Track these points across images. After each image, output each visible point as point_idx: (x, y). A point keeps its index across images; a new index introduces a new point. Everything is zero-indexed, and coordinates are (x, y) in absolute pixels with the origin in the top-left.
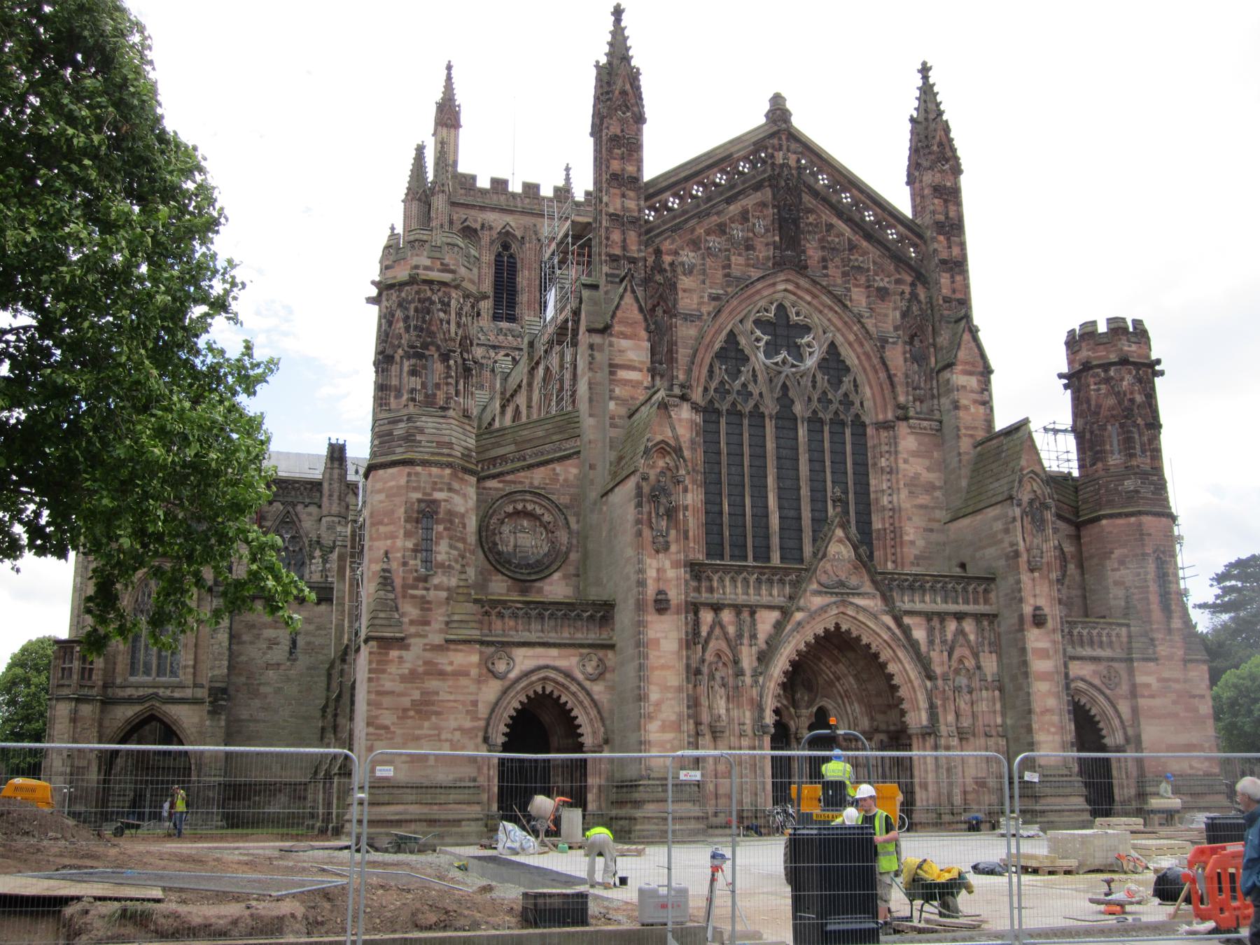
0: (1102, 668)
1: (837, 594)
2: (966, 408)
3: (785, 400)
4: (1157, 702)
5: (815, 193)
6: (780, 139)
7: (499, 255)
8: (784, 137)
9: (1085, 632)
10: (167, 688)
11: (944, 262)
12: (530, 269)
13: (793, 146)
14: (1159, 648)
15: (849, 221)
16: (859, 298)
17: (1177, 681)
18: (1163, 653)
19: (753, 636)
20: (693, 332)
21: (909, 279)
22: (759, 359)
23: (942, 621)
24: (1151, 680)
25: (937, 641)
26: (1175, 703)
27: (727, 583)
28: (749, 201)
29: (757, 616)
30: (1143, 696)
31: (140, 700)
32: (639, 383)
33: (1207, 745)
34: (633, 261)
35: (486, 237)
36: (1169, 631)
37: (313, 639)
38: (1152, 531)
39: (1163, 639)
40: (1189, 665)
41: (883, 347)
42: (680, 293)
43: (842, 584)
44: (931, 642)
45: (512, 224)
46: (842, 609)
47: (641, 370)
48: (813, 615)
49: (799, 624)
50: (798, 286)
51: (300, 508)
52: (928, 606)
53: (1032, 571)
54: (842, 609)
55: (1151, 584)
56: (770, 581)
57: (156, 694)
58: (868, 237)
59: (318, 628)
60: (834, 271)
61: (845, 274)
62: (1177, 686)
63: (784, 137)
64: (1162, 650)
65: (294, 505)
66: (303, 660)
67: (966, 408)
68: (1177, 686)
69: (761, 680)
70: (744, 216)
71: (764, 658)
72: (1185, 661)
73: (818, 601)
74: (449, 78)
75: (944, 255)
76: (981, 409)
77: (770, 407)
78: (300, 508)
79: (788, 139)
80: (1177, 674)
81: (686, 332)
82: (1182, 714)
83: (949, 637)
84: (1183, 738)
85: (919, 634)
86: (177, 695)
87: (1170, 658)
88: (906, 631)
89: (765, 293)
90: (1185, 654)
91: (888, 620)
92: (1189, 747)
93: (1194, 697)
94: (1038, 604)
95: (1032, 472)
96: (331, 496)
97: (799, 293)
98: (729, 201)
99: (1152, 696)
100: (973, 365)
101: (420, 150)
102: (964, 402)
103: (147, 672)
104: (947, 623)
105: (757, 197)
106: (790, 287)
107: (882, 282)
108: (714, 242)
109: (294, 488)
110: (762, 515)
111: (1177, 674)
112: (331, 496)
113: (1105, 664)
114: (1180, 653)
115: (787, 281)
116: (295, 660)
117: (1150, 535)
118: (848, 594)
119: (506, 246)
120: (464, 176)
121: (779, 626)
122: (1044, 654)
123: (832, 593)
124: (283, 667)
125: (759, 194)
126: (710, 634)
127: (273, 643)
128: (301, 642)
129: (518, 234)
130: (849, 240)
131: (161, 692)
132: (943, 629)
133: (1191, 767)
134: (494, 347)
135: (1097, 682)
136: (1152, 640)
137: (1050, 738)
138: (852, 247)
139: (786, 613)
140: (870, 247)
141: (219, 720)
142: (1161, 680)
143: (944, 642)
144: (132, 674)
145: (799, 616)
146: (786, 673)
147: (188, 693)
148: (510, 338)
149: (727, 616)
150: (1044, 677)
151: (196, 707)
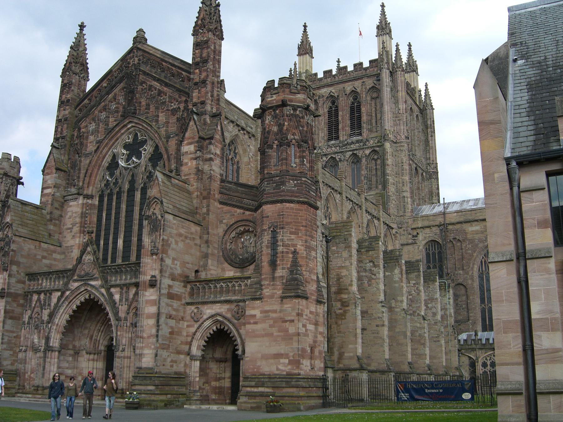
0: (233, 306)
1: (84, 280)
2: (187, 164)
3: (132, 182)
4: (259, 327)
5: (145, 73)
6: (134, 52)
7: (331, 108)
8: (135, 51)
9: (224, 285)
11: (196, 84)
12: (342, 111)
13: (140, 53)
14: (265, 291)
15: (158, 80)
16: (162, 118)
17: (275, 311)
18: (267, 294)
19: (49, 305)
20: (88, 162)
21: (184, 99)
22: (122, 163)
23: (128, 288)
24: (257, 312)
25: (124, 300)
26: (271, 326)
27: (45, 281)
28: (116, 90)
29: (53, 294)
30: (250, 323)
32: (50, 193)
33: (291, 354)
34: (63, 138)
36: (273, 279)
38: (269, 214)
39: (268, 284)
40: (284, 300)
41: (167, 141)
42: (89, 145)
43: (87, 274)
44: (121, 300)
45: (333, 91)
46: (86, 288)
47: (51, 188)
48: (73, 292)
49: (67, 298)
50: (136, 123)
52: (123, 282)
53: (152, 254)
54: (86, 288)
55: (264, 249)
56: (59, 278)
58: (167, 85)
60: (152, 108)
61: (157, 108)
62: (274, 315)
63: (135, 51)
64: (266, 292)
67: (187, 164)
68: (274, 315)
69: (50, 325)
70: (115, 98)
71: (51, 316)
72: (283, 298)
73: (76, 284)
74: (305, 31)
75: (197, 80)
76: (194, 162)
77: (127, 186)
79: (137, 52)
80: (276, 307)
81: (85, 162)
82: (275, 334)
83: (131, 296)
84: (274, 350)
85: (117, 297)
87: (272, 296)
88: (111, 295)
89: (122, 131)
90: (283, 293)
91: (103, 290)
92: (278, 356)
93: (286, 321)
94: (154, 274)
95: (155, 198)
97: (137, 126)
98: (108, 93)
99: (256, 323)
100: (193, 138)
102: (185, 161)
104: (130, 288)
105: (122, 85)
106: (133, 125)
107: (174, 106)
108: (103, 115)
110: (115, 243)
111: (276, 307)
113: (236, 304)
114: (279, 292)
115: (130, 122)
117: (268, 217)
118: (88, 280)
121: (59, 299)
122: (153, 303)
123: (81, 280)
125: (122, 84)
126: (35, 305)
129: (336, 95)
130: (159, 90)
132: (127, 292)
133: (278, 369)
135: (229, 315)
136: (262, 286)
137: (151, 351)
138: (160, 93)
139: (63, 293)
140: (168, 90)
142: (262, 312)
143: (127, 300)
145: (68, 293)
146: (68, 322)
148: (334, 148)
149: (42, 296)
150: (149, 316)
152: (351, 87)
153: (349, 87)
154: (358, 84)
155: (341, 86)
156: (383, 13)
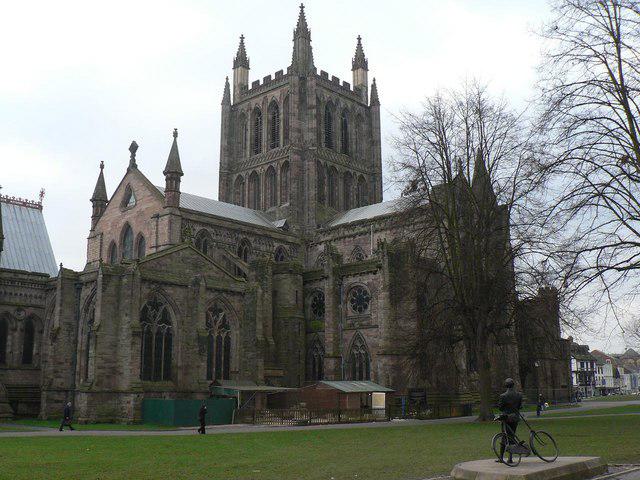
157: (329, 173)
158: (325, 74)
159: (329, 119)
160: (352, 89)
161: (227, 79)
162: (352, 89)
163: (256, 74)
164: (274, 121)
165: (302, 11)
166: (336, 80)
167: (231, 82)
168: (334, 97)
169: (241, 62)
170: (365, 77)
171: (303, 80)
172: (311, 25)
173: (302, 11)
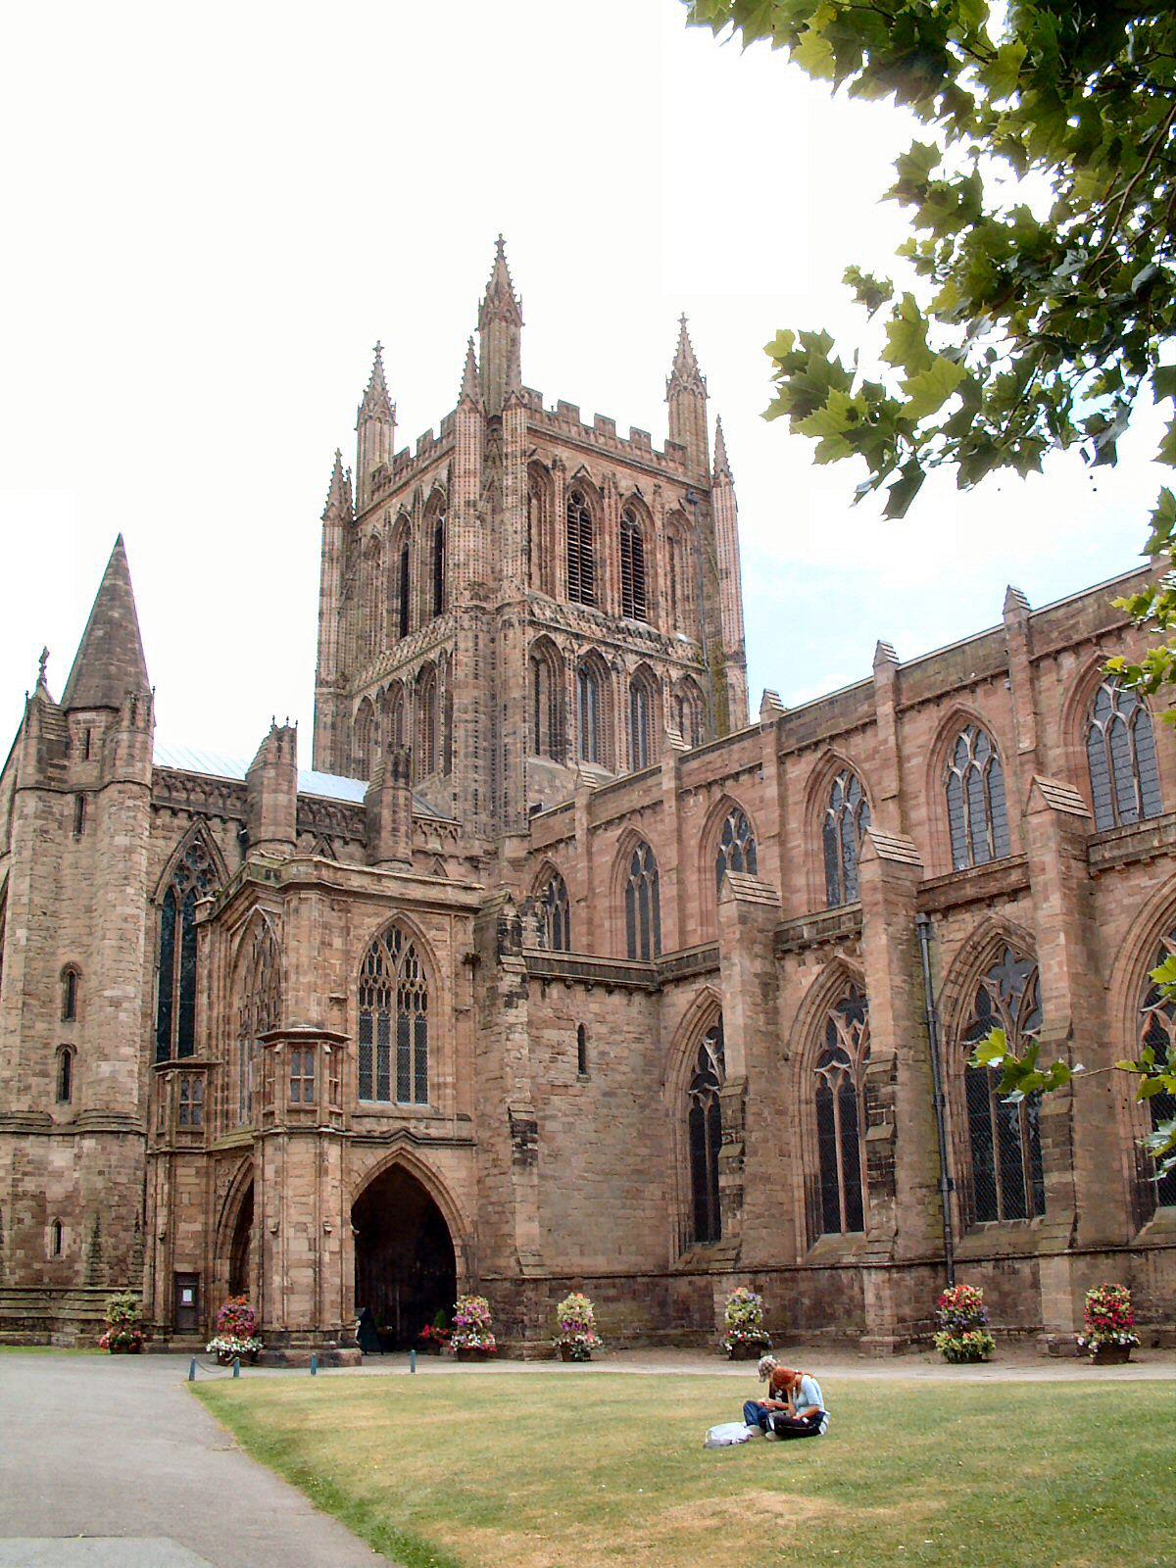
10: (419, 1120)
31: (384, 1140)
35: (558, 480)
37: (607, 1048)
45: (589, 469)
51: (337, 844)
57: (406, 1130)
59: (613, 1031)
65: (330, 838)
66: (597, 1081)
78: (337, 844)
86: (434, 1132)
96: (395, 830)
101: (471, 343)
103: (383, 1095)
109: (328, 814)
112: (395, 830)
116: (588, 1080)
119: (577, 498)
120: (529, 392)
124: (571, 1091)
127: (558, 1052)
128: (592, 1052)
129: (597, 482)
131: (411, 1125)
134: (577, 636)
141: (531, 1174)
144: (365, 1092)
147: (449, 1130)
148: (593, 626)
151: (461, 1152)
152: (631, 483)
153: (626, 481)
154: (646, 483)
155: (607, 467)
156: (684, 335)
157: (584, 674)
158: (568, 411)
159: (582, 527)
160: (658, 445)
161: (339, 454)
162: (658, 445)
163: (405, 438)
164: (440, 538)
165: (500, 251)
166: (604, 424)
167: (350, 461)
168: (597, 471)
169: (376, 410)
170: (699, 417)
171: (493, 422)
172: (522, 288)
173: (500, 251)
